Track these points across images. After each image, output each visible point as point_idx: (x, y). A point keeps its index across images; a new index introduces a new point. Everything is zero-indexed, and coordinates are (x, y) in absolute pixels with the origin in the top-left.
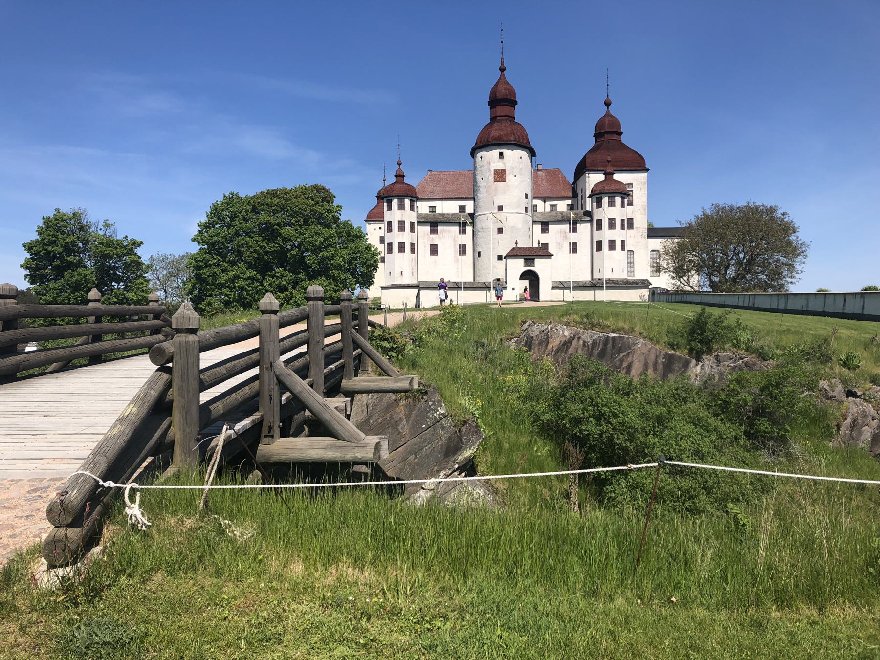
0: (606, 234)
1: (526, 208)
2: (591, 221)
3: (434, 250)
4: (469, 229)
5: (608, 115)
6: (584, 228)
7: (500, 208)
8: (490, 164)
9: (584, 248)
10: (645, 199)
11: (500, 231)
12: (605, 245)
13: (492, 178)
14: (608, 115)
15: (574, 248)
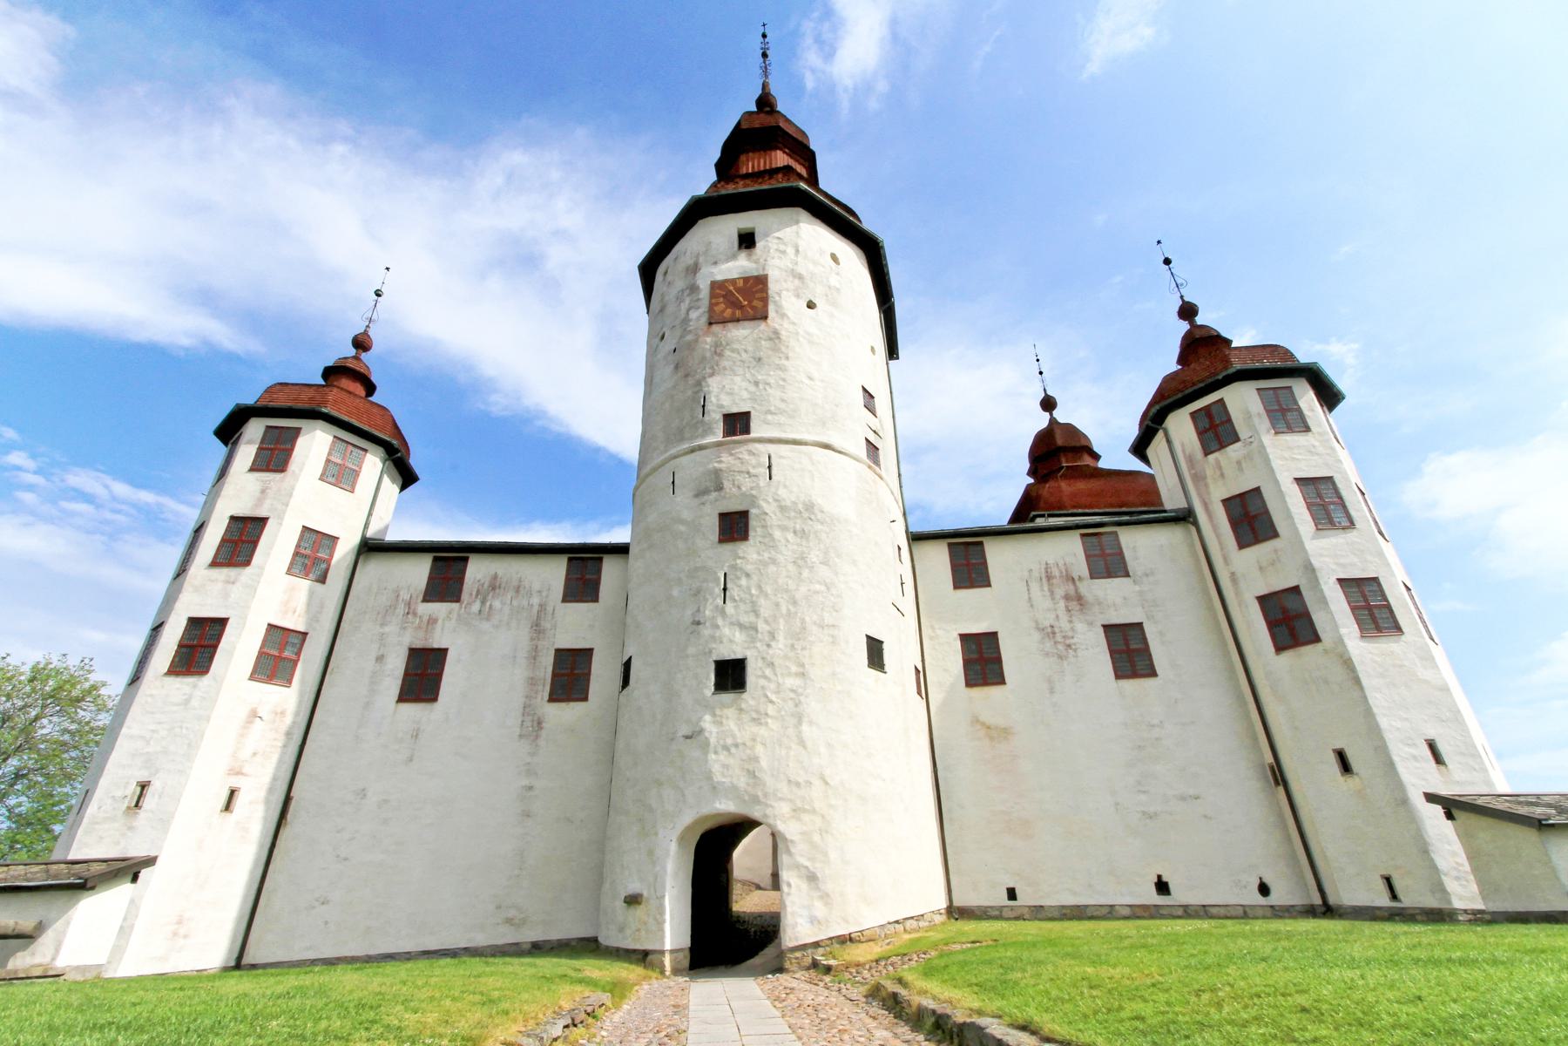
1: (872, 449)
3: (423, 675)
5: (1053, 421)
8: (694, 269)
13: (698, 316)
14: (1053, 421)
15: (1129, 652)
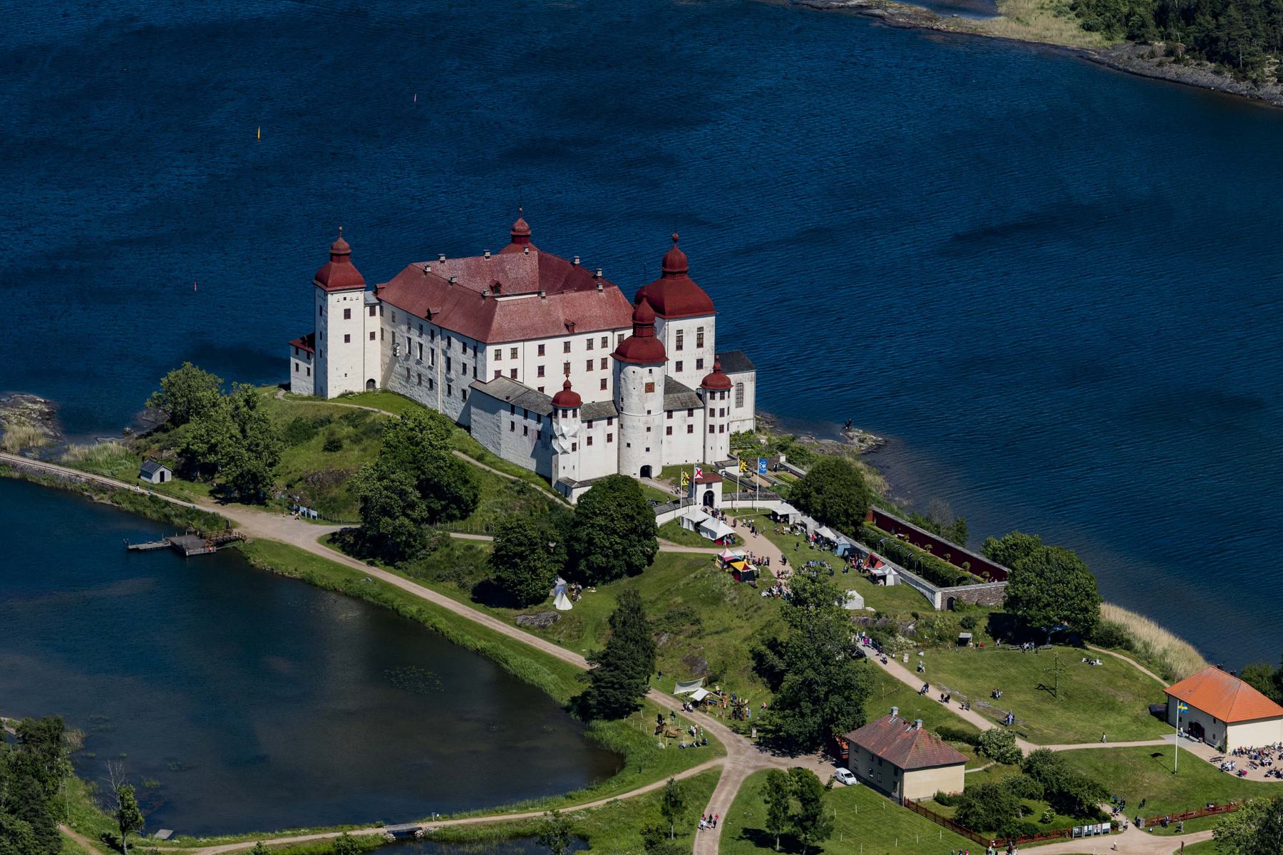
0: (717, 421)
2: (704, 408)
4: (615, 421)
6: (698, 413)
7: (649, 412)
9: (699, 429)
10: (713, 340)
11: (649, 429)
12: (717, 429)
15: (690, 429)
